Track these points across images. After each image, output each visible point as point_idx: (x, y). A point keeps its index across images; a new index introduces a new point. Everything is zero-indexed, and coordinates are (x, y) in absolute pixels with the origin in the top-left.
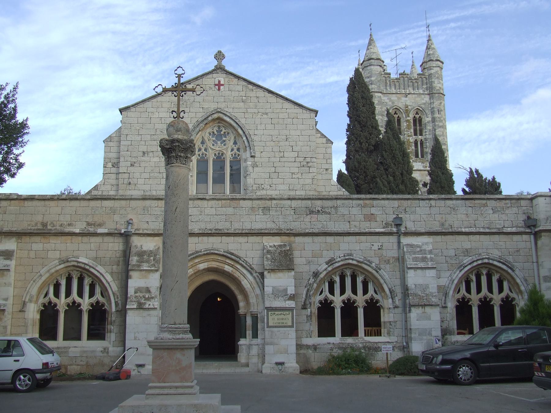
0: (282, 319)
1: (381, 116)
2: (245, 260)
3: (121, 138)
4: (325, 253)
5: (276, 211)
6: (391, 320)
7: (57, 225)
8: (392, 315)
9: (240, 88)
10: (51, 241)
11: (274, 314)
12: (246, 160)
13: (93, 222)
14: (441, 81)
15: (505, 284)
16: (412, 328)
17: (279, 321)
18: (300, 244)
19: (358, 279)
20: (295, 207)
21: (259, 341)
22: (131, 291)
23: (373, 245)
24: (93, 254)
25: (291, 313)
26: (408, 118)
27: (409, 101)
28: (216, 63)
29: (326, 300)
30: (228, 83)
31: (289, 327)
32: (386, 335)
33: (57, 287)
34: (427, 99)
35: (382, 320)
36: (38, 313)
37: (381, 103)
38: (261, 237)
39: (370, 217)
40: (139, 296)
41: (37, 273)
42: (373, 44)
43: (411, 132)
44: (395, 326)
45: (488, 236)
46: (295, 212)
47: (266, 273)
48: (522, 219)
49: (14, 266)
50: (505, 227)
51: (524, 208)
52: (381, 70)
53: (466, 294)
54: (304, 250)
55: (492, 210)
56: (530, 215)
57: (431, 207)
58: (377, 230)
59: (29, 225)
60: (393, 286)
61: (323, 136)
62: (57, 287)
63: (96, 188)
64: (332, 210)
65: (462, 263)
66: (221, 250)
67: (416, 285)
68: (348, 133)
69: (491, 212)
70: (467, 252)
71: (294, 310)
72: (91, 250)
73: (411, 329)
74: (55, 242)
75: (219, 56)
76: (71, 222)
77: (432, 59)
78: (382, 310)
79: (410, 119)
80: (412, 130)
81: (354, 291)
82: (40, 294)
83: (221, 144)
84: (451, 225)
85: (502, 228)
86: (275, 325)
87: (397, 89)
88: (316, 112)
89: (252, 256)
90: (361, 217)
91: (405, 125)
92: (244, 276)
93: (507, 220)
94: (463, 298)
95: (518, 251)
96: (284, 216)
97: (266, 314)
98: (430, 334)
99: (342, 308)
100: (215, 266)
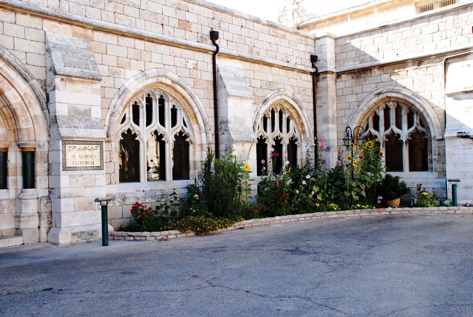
0: (86, 156)
2: (11, 53)
11: (74, 147)
18: (101, 44)
23: (188, 62)
25: (99, 148)
35: (191, 159)
38: (40, 19)
53: (264, 132)
54: (107, 54)
57: (242, 26)
58: (194, 43)
65: (266, 98)
70: (270, 85)
71: (104, 143)
81: (162, 122)
90: (174, 22)
92: (9, 82)
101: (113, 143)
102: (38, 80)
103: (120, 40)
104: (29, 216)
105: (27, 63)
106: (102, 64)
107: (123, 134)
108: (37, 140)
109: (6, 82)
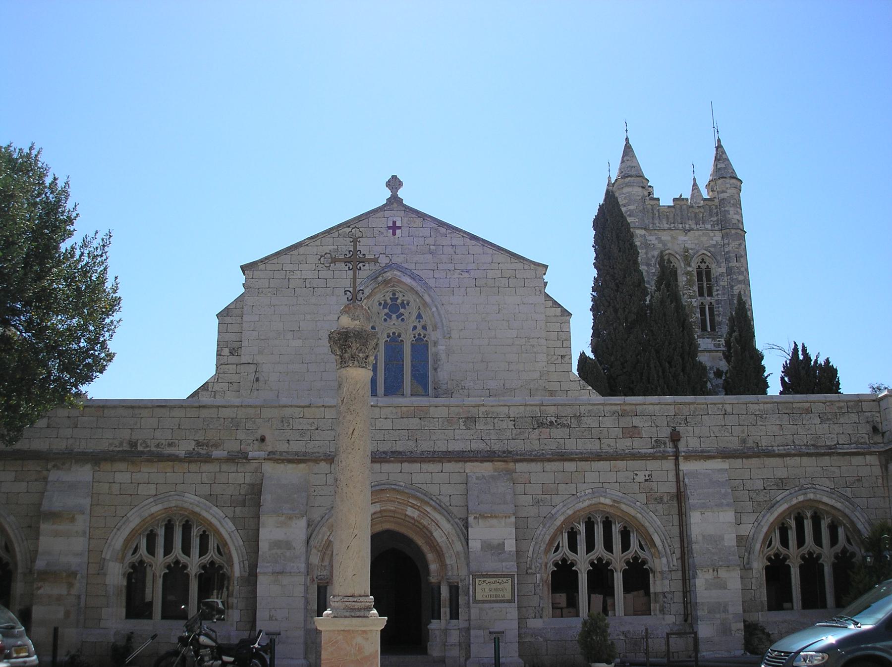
0: (497, 590)
1: (646, 265)
2: (437, 499)
3: (245, 309)
4: (562, 487)
5: (486, 424)
6: (665, 590)
7: (153, 445)
8: (667, 582)
9: (426, 232)
10: (144, 469)
11: (484, 581)
12: (435, 344)
13: (205, 441)
14: (738, 210)
15: (841, 531)
16: (698, 601)
17: (492, 593)
18: (523, 474)
19: (613, 527)
20: (514, 417)
21: (461, 623)
22: (263, 546)
23: (637, 475)
24: (206, 490)
25: (510, 581)
26: (689, 269)
27: (690, 242)
28: (388, 194)
29: (564, 560)
30: (407, 225)
31: (509, 601)
32: (658, 612)
33: (151, 538)
34: (717, 237)
35: (652, 590)
36: (124, 577)
37: (647, 245)
39: (632, 432)
40: (277, 553)
41: (123, 517)
42: (630, 154)
43: (694, 291)
44: (671, 599)
45: (814, 458)
46: (514, 425)
47: (471, 519)
48: (864, 431)
49: (89, 505)
50: (839, 444)
51: (866, 413)
52: (644, 195)
55: (820, 418)
56: (876, 425)
59: (110, 445)
60: (668, 537)
61: (556, 304)
62: (151, 538)
63: (205, 387)
64: (572, 421)
66: (402, 484)
67: (704, 536)
68: (593, 293)
69: (818, 421)
70: (781, 484)
71: (516, 576)
72: (202, 483)
73: (696, 603)
74: (147, 472)
75: (394, 183)
76: (172, 441)
77: (725, 176)
78: (651, 575)
79: (692, 271)
80: (696, 288)
81: (609, 546)
82: (127, 549)
83: (398, 318)
84: (756, 441)
85: (835, 445)
86: (486, 599)
87: (671, 224)
88: (546, 267)
89: (450, 492)
91: (685, 279)
92: (437, 524)
93: (843, 433)
94: (777, 555)
95: (858, 480)
96: (498, 431)
97: (471, 582)
98: (726, 611)
99: (589, 572)
100: (392, 508)
101: (537, 575)
102: (459, 519)
103: (546, 466)
104: (451, 645)
105: (450, 505)
106: (525, 494)
107: (556, 564)
108: (460, 575)
109: (433, 523)
